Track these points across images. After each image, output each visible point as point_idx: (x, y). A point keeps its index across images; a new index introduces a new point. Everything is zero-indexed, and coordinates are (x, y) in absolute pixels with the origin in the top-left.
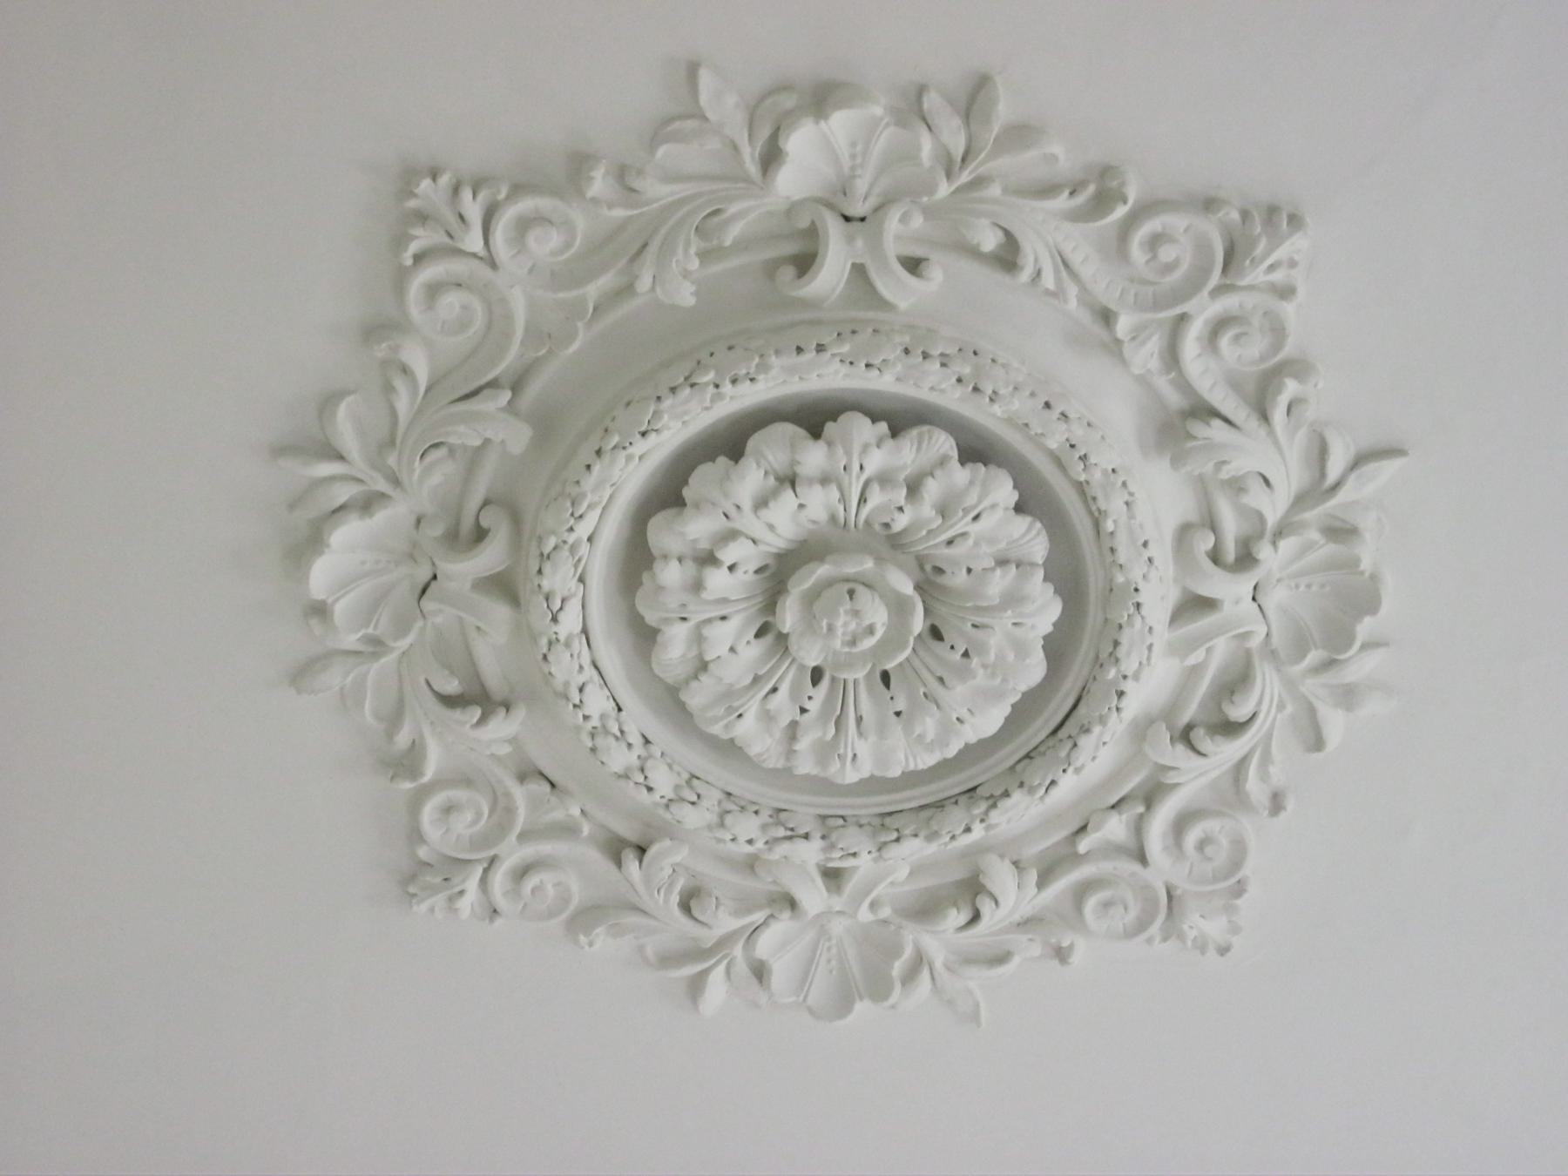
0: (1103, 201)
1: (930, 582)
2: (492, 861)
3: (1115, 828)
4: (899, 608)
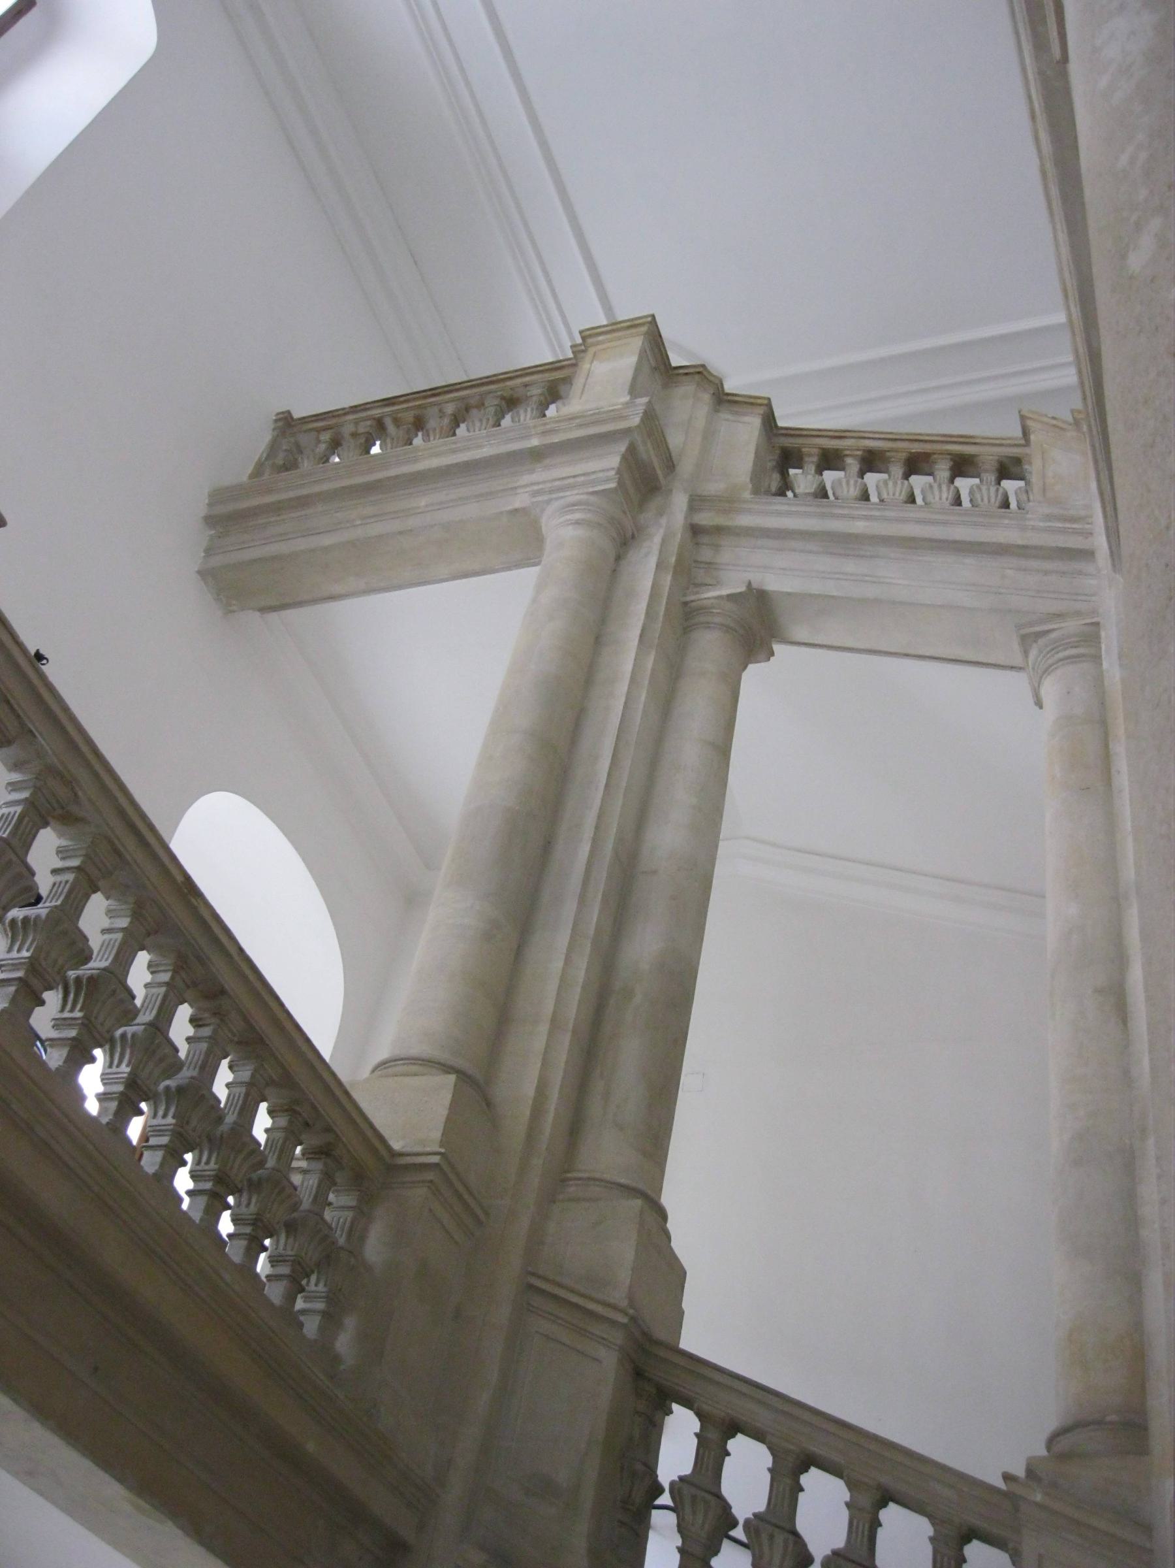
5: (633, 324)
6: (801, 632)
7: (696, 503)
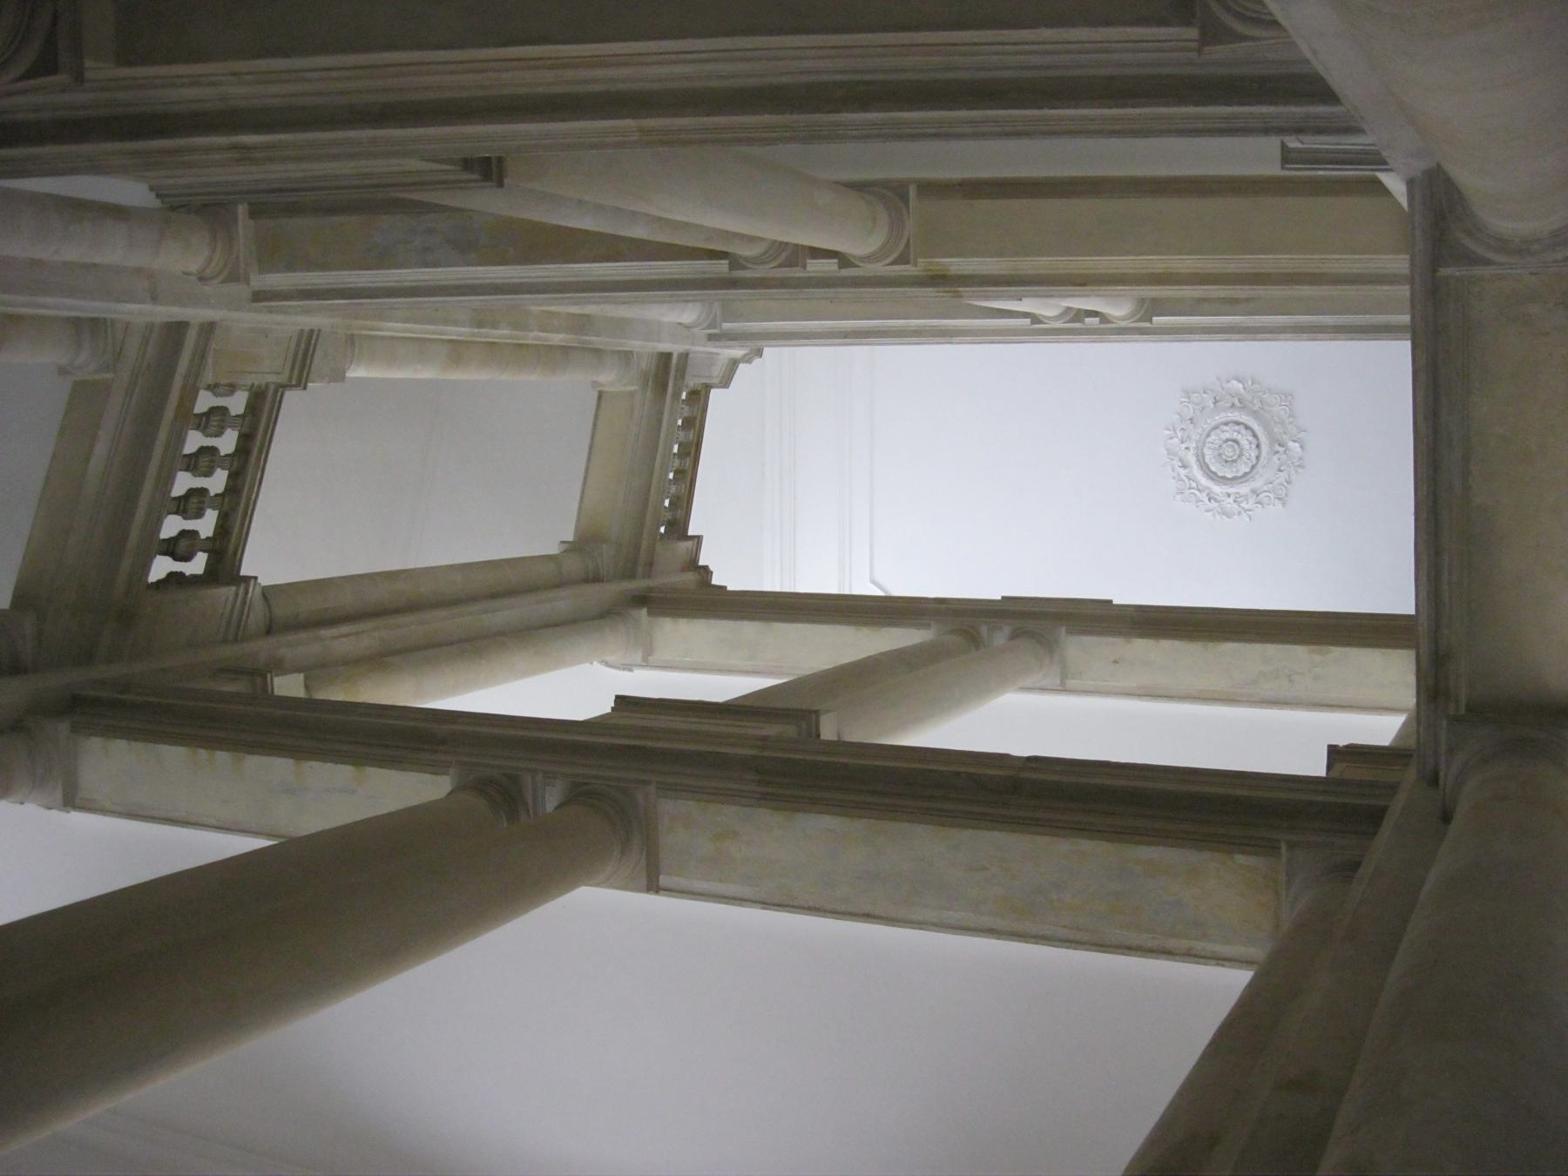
0: (1287, 482)
1: (1235, 461)
3: (1194, 485)
4: (1231, 457)
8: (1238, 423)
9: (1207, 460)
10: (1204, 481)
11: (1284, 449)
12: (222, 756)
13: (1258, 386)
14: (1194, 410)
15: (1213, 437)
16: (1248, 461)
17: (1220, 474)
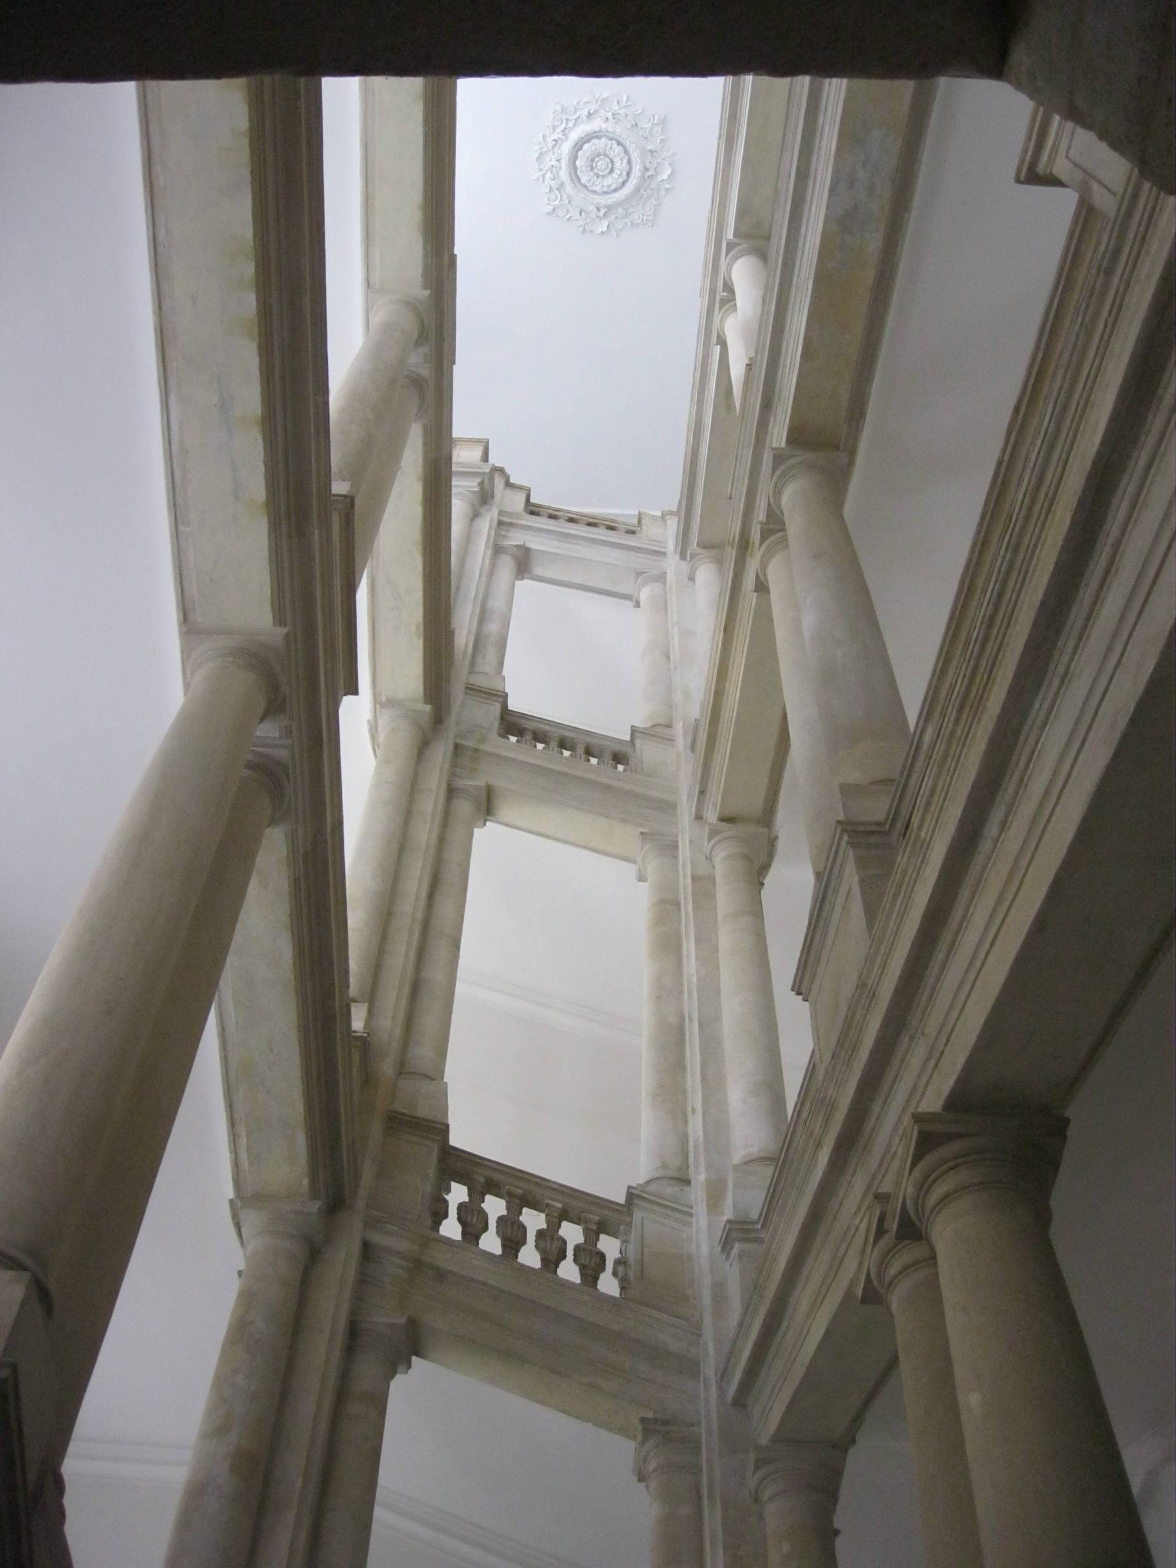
1: (592, 169)
2: (652, 124)
3: (571, 124)
5: (478, 441)
6: (538, 571)
7: (501, 513)
8: (628, 174)
9: (594, 141)
10: (574, 136)
11: (602, 216)
12: (249, 302)
13: (663, 194)
14: (647, 128)
15: (618, 149)
16: (591, 184)
17: (580, 153)
